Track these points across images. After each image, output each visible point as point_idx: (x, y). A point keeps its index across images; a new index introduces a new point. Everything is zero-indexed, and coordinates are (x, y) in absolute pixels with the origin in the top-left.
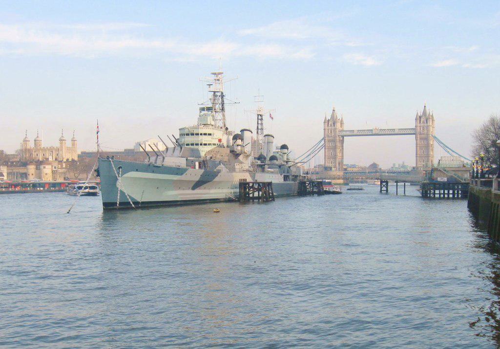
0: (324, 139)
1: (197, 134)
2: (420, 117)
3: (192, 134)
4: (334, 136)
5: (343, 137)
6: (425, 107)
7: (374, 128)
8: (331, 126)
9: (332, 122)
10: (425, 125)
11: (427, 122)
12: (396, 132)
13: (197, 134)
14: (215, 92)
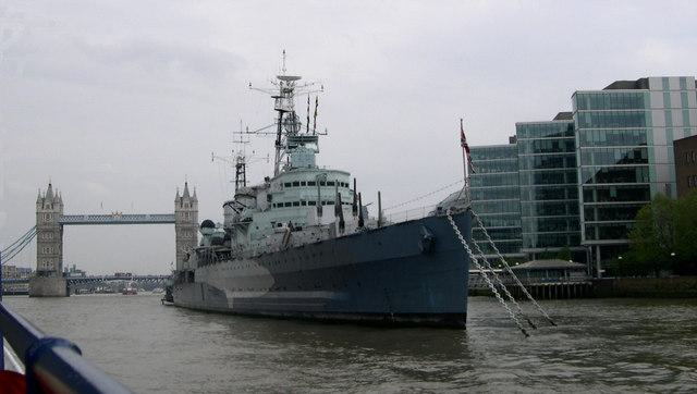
5: (62, 225)
8: (48, 207)
12: (147, 219)
14: (282, 112)
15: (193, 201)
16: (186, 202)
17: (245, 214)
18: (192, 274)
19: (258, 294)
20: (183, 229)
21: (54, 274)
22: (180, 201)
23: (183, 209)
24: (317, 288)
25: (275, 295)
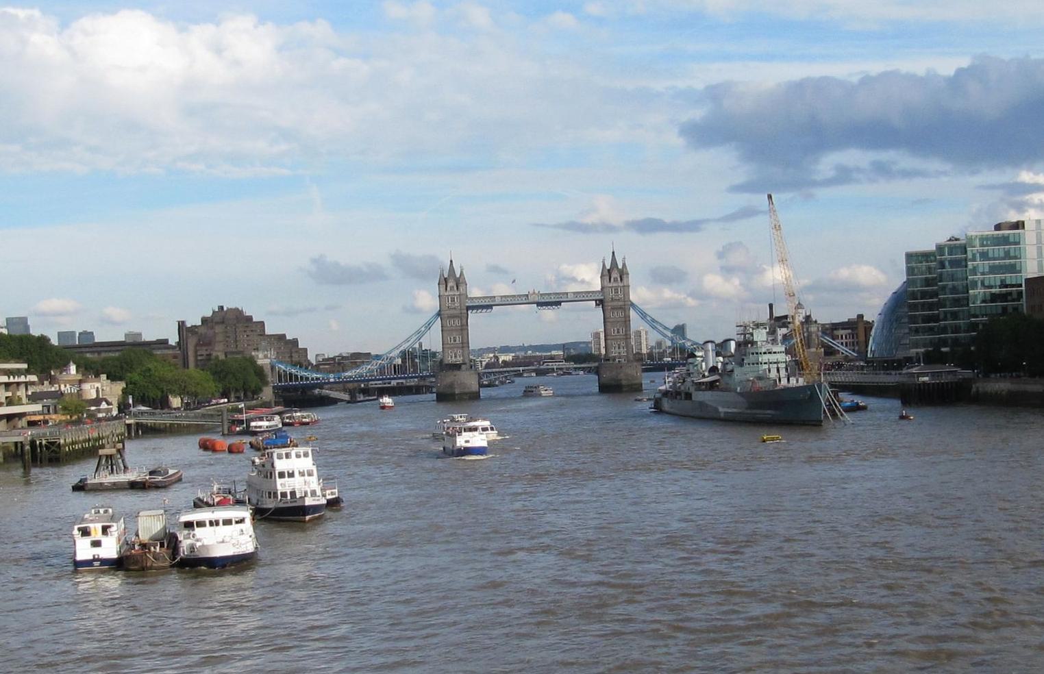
0: (439, 314)
1: (775, 353)
2: (609, 270)
3: (770, 353)
4: (457, 307)
6: (613, 253)
7: (531, 292)
8: (452, 288)
9: (451, 281)
10: (621, 284)
11: (621, 280)
12: (570, 297)
13: (775, 353)
15: (623, 274)
16: (614, 273)
17: (729, 367)
18: (691, 394)
19: (740, 411)
20: (613, 308)
21: (463, 367)
22: (607, 274)
23: (613, 284)
24: (770, 409)
25: (749, 411)
